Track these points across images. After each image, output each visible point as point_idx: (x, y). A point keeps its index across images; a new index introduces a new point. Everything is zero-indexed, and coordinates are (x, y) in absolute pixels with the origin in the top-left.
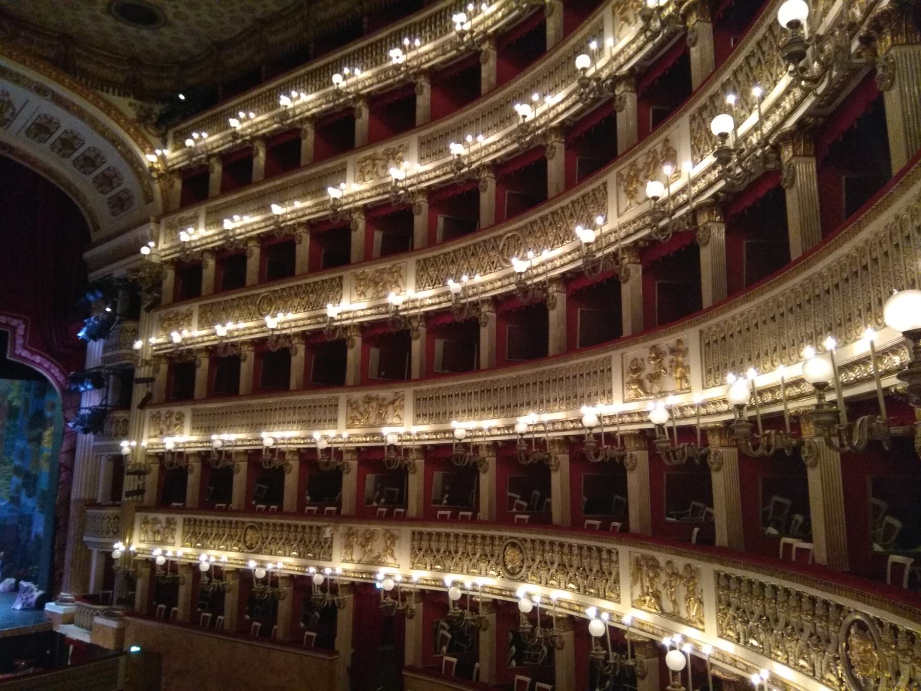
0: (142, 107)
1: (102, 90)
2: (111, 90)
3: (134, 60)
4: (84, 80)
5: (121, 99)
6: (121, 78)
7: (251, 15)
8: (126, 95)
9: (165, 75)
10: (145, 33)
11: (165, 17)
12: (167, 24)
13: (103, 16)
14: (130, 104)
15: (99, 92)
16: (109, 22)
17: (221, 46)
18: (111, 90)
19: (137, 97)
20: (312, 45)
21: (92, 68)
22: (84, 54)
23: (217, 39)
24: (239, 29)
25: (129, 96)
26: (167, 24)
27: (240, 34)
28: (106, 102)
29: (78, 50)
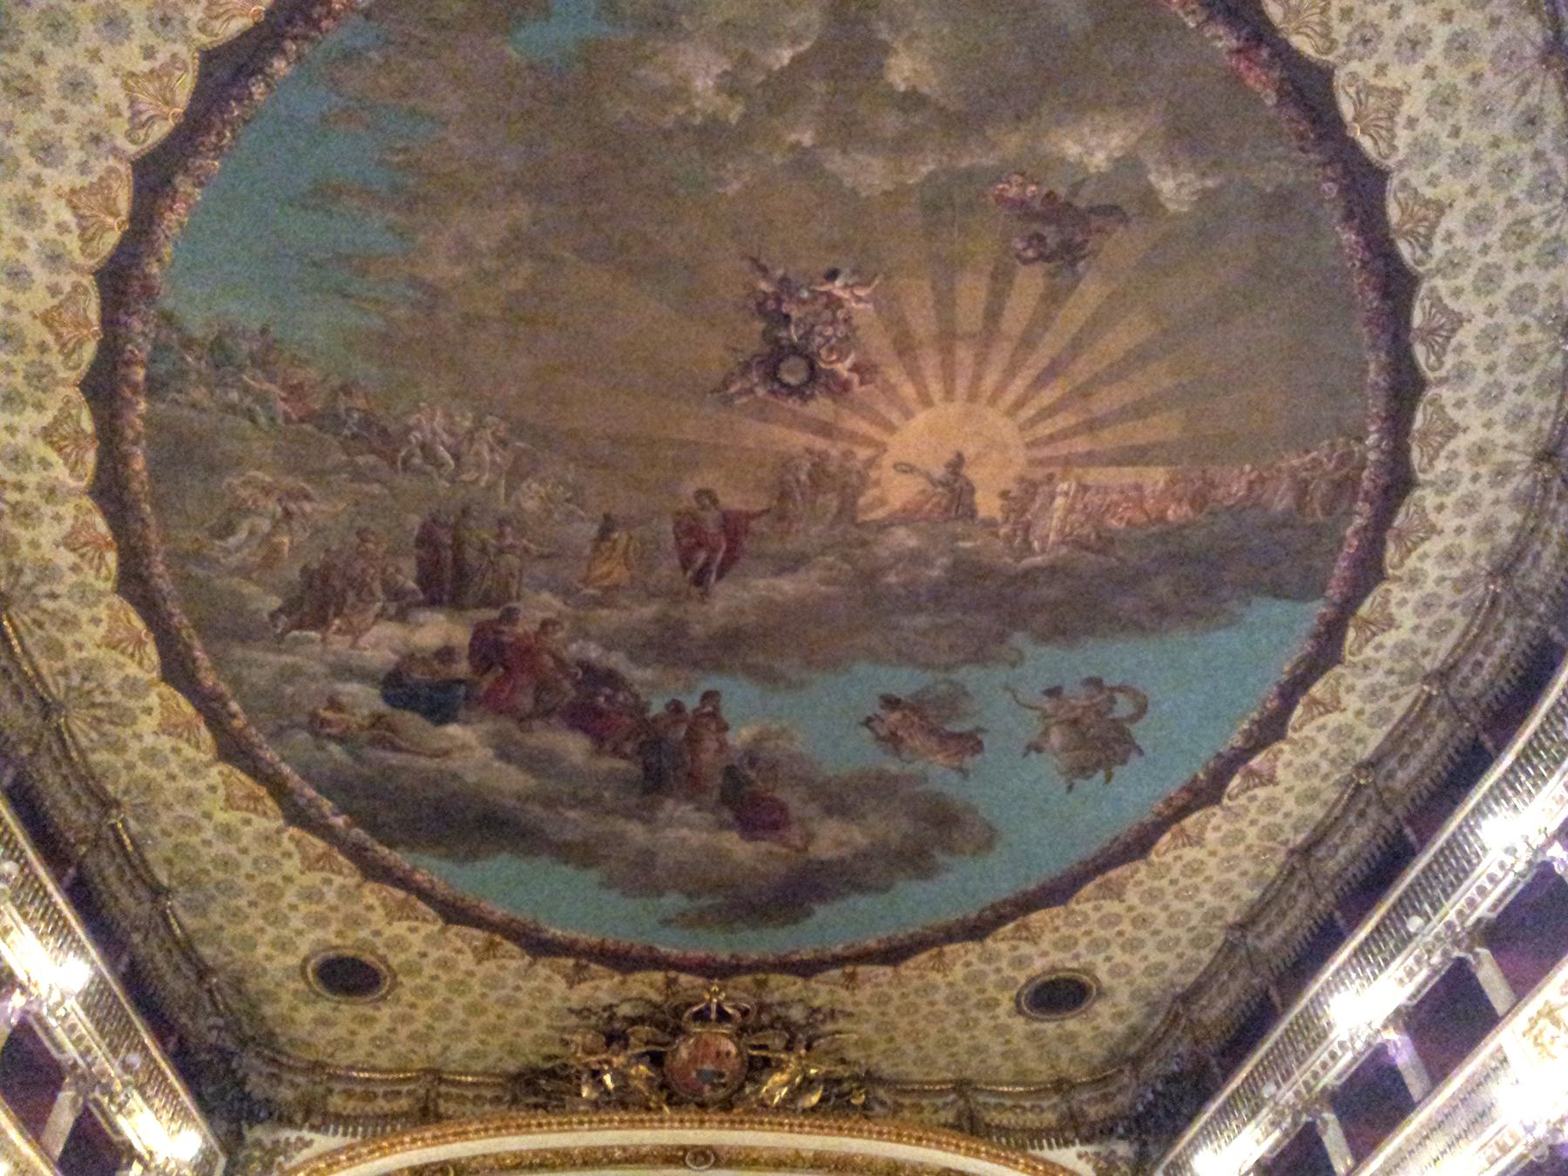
0: (1097, 1154)
1: (1033, 1147)
2: (1045, 1142)
3: (1061, 1085)
4: (1004, 1140)
5: (1064, 1150)
6: (1050, 1118)
7: (1218, 923)
8: (1068, 1143)
9: (1112, 1089)
10: (1072, 1025)
11: (1097, 980)
12: (1101, 994)
13: (1010, 1021)
14: (1080, 1156)
15: (1030, 1151)
16: (1019, 1025)
17: (1188, 997)
18: (1045, 1142)
19: (1087, 1140)
20: (1338, 914)
21: (1006, 1119)
22: (993, 1101)
23: (1179, 990)
24: (1206, 955)
25: (1073, 1144)
26: (1101, 994)
27: (1212, 962)
28: (1045, 1162)
29: (981, 1099)
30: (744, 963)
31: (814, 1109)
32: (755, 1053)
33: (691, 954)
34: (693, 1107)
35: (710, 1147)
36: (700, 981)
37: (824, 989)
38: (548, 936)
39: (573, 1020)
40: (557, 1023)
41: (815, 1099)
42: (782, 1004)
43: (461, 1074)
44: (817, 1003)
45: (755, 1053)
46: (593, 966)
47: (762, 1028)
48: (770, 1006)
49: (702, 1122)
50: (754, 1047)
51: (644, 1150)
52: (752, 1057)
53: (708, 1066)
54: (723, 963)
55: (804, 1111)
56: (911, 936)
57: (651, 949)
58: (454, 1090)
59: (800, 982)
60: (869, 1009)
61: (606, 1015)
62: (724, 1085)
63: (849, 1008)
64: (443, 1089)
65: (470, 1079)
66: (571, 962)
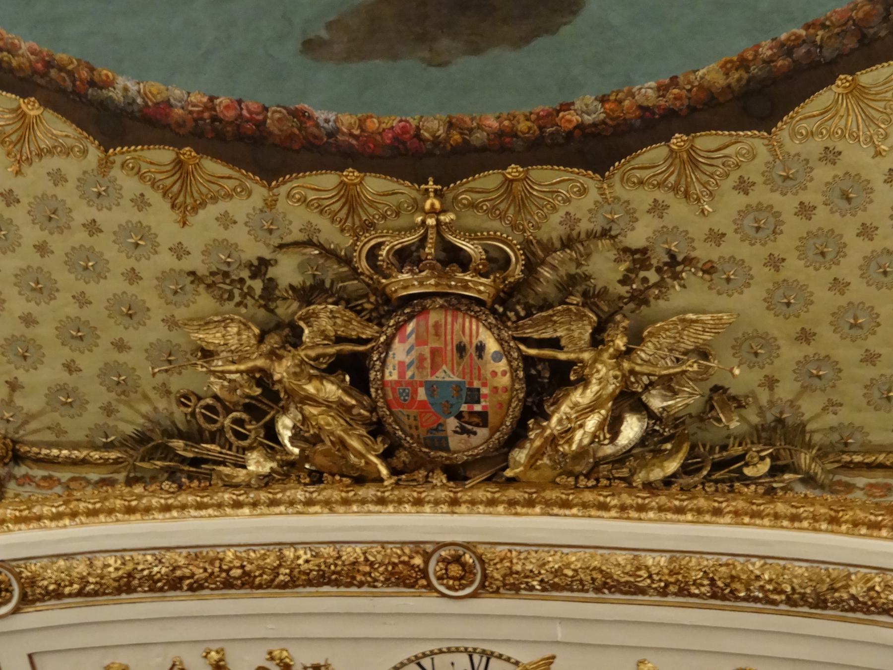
30: (479, 138)
31: (668, 482)
32: (533, 352)
33: (373, 124)
34: (440, 478)
35: (468, 546)
36: (405, 190)
37: (643, 198)
38: (116, 94)
39: (205, 302)
40: (181, 313)
41: (672, 466)
42: (568, 243)
43: (50, 445)
44: (636, 238)
45: (533, 352)
46: (213, 167)
47: (546, 305)
48: (549, 248)
49: (454, 502)
50: (529, 342)
51: (350, 553)
52: (528, 361)
53: (446, 375)
54: (436, 141)
55: (648, 486)
56: (786, 49)
57: (300, 115)
58: (39, 473)
59: (589, 180)
60: (744, 251)
61: (258, 285)
62: (483, 419)
63: (704, 252)
64: (21, 470)
65: (65, 452)
66: (164, 155)
